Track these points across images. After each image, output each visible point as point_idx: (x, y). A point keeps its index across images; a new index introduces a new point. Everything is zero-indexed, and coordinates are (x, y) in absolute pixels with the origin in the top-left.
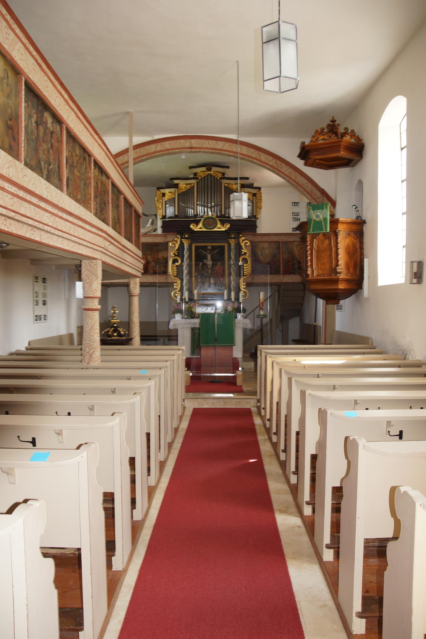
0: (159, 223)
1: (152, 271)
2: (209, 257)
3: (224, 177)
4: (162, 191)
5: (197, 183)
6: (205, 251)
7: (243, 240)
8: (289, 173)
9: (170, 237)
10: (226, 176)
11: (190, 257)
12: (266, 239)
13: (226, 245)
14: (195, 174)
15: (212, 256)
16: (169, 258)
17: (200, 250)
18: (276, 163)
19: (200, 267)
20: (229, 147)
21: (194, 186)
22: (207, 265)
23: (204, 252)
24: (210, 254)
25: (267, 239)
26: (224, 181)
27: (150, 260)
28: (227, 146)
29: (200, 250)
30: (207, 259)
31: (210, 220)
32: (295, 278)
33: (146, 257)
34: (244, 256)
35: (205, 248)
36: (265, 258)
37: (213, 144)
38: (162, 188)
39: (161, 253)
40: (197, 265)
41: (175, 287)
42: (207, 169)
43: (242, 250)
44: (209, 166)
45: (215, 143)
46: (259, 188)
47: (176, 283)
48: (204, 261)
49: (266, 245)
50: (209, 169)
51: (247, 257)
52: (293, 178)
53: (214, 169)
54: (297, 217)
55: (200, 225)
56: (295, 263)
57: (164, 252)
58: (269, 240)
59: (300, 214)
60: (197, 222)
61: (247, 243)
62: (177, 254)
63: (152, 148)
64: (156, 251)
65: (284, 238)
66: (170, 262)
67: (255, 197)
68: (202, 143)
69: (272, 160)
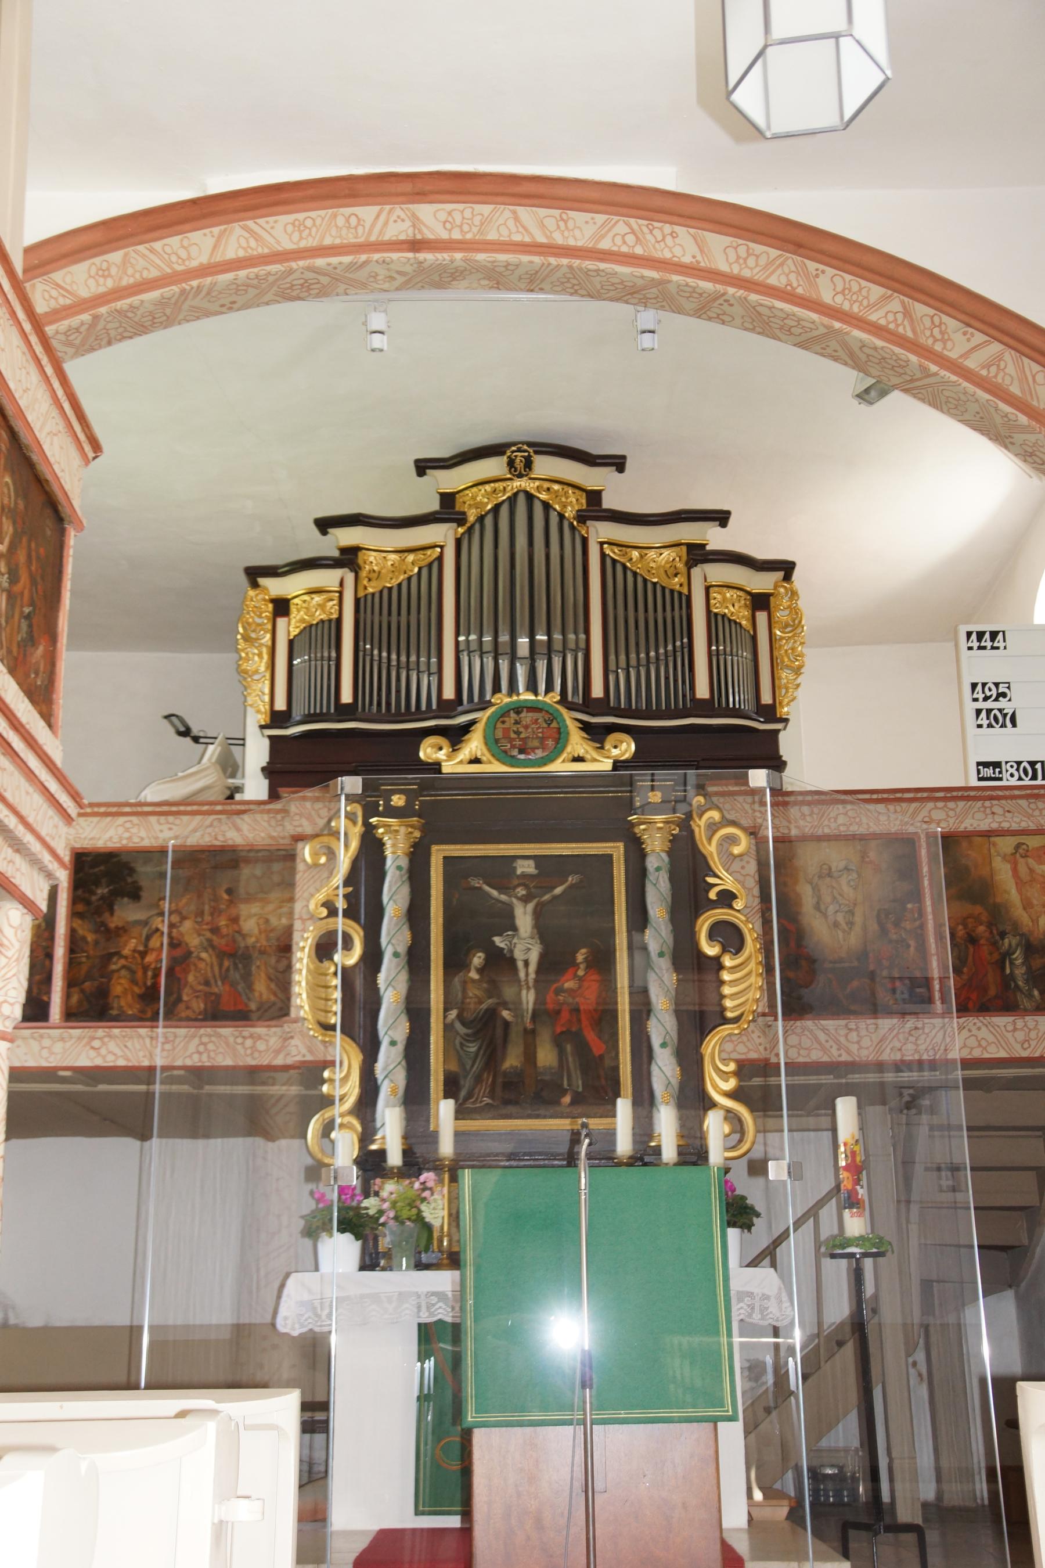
1: (199, 1005)
2: (524, 918)
3: (594, 506)
4: (276, 587)
5: (458, 542)
6: (501, 889)
7: (713, 828)
8: (988, 367)
9: (304, 809)
11: (416, 914)
12: (840, 819)
13: (617, 850)
14: (448, 499)
15: (537, 914)
16: (298, 925)
17: (476, 883)
18: (907, 313)
19: (474, 975)
20: (630, 239)
21: (440, 559)
22: (512, 961)
23: (495, 893)
24: (530, 906)
25: (841, 820)
26: (601, 531)
27: (194, 941)
28: (618, 233)
29: (476, 883)
30: (515, 929)
31: (527, 717)
32: (1020, 1035)
34: (720, 914)
35: (500, 872)
37: (542, 226)
38: (272, 572)
39: (255, 908)
42: (511, 463)
44: (519, 453)
45: (550, 223)
46: (787, 568)
48: (497, 940)
49: (836, 856)
50: (519, 464)
51: (738, 919)
52: (1015, 389)
53: (546, 466)
54: (1003, 703)
55: (474, 744)
56: (1009, 953)
58: (854, 829)
59: (1012, 694)
60: (456, 736)
61: (732, 840)
63: (199, 246)
64: (229, 891)
65: (938, 815)
66: (303, 958)
67: (762, 617)
68: (477, 220)
69: (885, 299)
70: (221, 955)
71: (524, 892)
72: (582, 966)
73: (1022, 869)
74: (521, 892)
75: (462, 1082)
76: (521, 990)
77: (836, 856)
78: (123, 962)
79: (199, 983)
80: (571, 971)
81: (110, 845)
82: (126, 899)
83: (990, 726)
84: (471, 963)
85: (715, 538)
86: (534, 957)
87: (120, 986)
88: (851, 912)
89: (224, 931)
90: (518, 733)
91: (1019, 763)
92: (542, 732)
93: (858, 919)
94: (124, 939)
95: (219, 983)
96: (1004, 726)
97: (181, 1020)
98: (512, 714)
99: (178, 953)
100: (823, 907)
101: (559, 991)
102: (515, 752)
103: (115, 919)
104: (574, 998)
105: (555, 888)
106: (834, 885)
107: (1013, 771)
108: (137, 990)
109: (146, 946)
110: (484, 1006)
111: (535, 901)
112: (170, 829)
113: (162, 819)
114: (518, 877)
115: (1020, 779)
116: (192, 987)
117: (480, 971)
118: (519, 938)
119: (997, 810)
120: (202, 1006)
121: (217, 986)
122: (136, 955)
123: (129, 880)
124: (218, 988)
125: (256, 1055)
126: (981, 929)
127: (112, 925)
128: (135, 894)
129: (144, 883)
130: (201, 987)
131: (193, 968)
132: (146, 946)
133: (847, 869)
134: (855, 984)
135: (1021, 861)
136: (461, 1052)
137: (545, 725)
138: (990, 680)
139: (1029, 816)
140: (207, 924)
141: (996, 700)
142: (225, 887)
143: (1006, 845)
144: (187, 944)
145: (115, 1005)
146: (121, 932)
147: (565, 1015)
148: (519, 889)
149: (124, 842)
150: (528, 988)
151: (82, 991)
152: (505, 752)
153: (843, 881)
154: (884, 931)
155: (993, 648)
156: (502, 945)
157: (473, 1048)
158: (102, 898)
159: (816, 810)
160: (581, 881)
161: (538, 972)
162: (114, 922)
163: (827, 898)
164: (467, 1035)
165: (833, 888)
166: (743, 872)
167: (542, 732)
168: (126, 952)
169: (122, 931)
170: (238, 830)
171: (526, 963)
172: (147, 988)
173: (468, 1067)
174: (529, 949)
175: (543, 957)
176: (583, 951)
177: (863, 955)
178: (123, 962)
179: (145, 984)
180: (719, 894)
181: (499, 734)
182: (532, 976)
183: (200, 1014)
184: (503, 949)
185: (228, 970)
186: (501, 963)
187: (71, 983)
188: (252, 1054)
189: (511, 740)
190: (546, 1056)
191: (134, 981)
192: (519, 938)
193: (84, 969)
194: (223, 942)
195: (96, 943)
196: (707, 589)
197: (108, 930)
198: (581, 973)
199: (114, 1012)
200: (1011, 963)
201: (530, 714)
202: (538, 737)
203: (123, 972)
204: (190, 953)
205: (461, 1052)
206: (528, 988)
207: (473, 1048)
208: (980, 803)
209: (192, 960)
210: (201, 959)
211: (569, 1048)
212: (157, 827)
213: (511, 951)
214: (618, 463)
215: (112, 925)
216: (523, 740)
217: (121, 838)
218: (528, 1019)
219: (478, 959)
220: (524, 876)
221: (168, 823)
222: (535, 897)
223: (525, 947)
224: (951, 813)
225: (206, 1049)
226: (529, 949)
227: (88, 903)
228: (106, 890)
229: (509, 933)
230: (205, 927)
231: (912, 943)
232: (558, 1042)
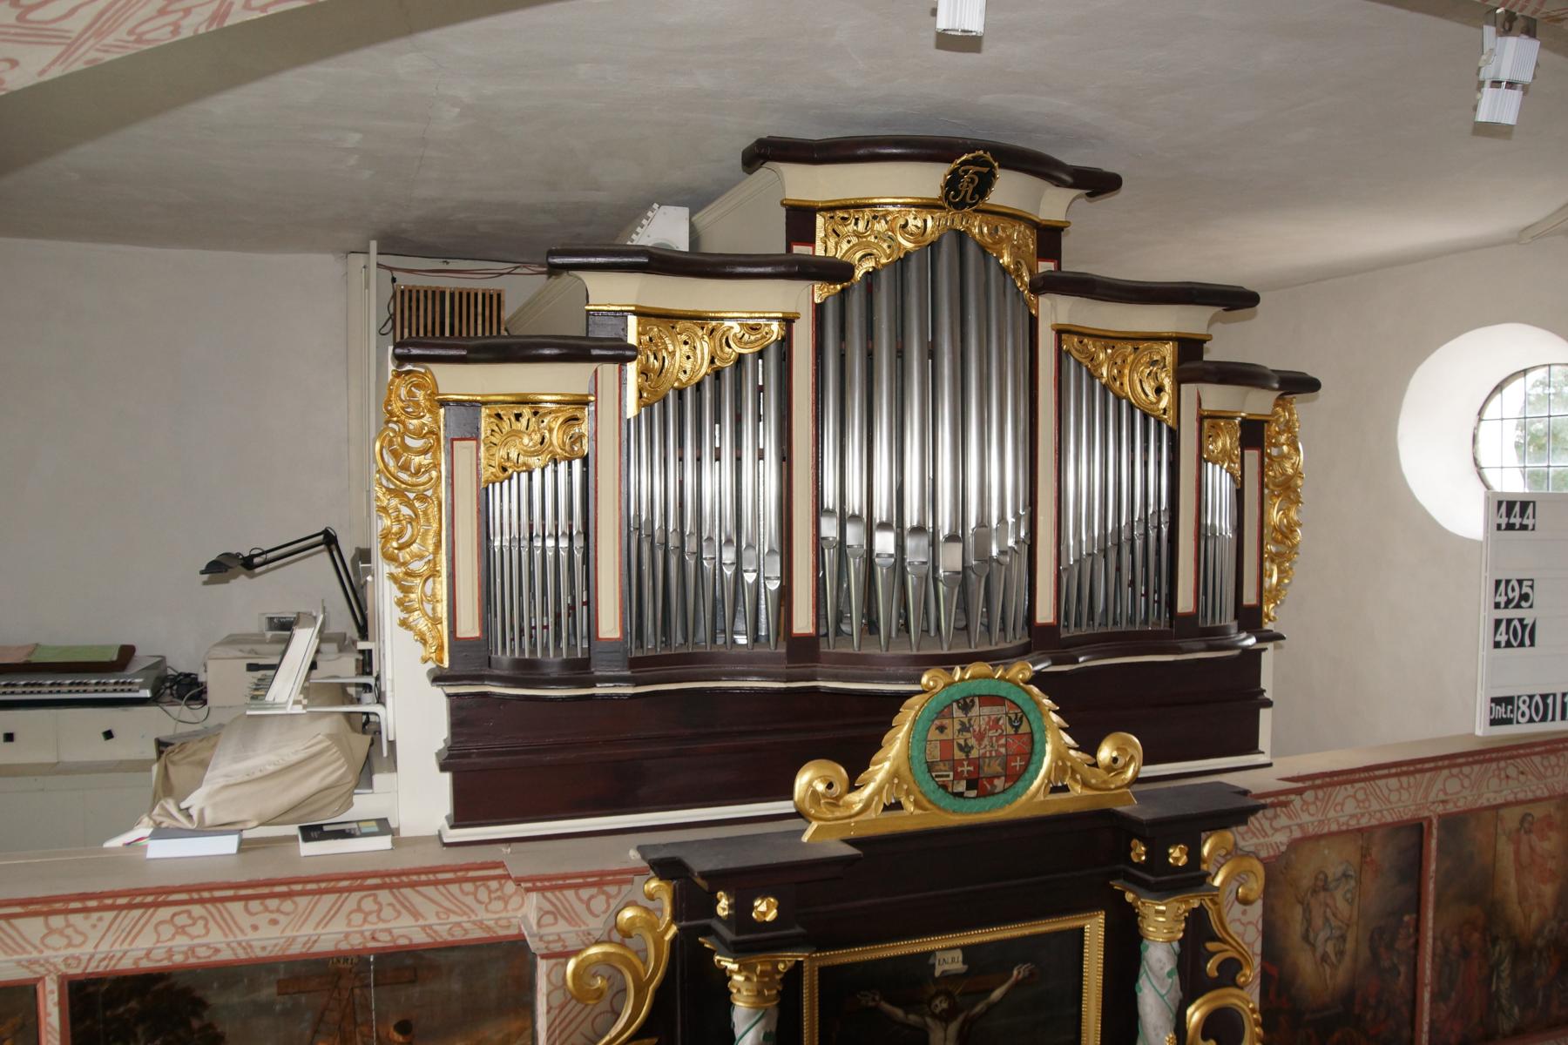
0: (417, 716)
5: (819, 310)
6: (908, 1004)
10: (1075, 260)
13: (1094, 927)
14: (800, 220)
23: (899, 1013)
25: (1350, 807)
31: (981, 715)
36: (1324, 958)
43: (1211, 946)
50: (966, 185)
53: (1008, 189)
59: (1536, 597)
65: (1453, 786)
67: (1252, 456)
71: (945, 1005)
73: (1525, 850)
77: (1334, 860)
81: (145, 964)
83: (1509, 644)
85: (1229, 341)
88: (1343, 938)
90: (966, 749)
91: (1531, 697)
92: (1005, 746)
93: (1350, 946)
96: (1522, 644)
98: (957, 713)
100: (1312, 935)
102: (961, 787)
105: (993, 990)
106: (1329, 901)
107: (1524, 708)
111: (961, 1018)
112: (274, 922)
113: (255, 905)
114: (936, 981)
115: (1531, 720)
119: (1512, 772)
123: (196, 1024)
126: (1476, 936)
133: (1345, 876)
135: (1525, 838)
137: (1011, 731)
138: (1514, 576)
139: (1541, 777)
141: (1518, 606)
142: (394, 1022)
143: (1511, 817)
149: (178, 959)
152: (944, 787)
153: (1339, 895)
154: (1375, 956)
155: (1524, 527)
159: (1320, 793)
160: (1032, 974)
163: (1318, 921)
165: (1327, 905)
166: (1245, 919)
167: (1005, 746)
170: (416, 915)
177: (1348, 997)
180: (1220, 967)
181: (936, 754)
189: (955, 765)
196: (1201, 419)
200: (1499, 977)
201: (986, 710)
202: (999, 755)
208: (1494, 765)
212: (245, 921)
214: (1098, 184)
216: (977, 764)
217: (170, 952)
220: (948, 977)
221: (267, 909)
224: (1466, 783)
231: (1402, 969)
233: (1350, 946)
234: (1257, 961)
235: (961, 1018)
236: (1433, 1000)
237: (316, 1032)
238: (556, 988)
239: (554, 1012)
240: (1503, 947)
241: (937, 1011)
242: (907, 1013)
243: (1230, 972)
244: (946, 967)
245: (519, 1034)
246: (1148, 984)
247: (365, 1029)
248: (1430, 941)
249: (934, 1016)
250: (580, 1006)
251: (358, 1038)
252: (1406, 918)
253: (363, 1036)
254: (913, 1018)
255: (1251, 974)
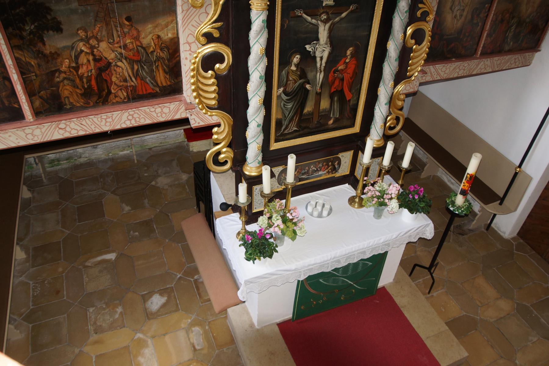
1: (123, 94)
2: (323, 33)
15: (331, 30)
17: (299, 13)
19: (293, 68)
22: (315, 57)
23: (309, 19)
24: (328, 25)
27: (111, 56)
29: (299, 13)
30: (318, 39)
33: (92, 48)
40: (285, 62)
41: (215, 137)
43: (420, 6)
47: (219, 125)
48: (308, 47)
57: (162, 21)
62: (216, 34)
64: (128, 19)
70: (131, 62)
71: (325, 17)
72: (349, 57)
74: (324, 17)
75: (283, 123)
76: (317, 73)
78: (63, 75)
79: (121, 81)
80: (343, 60)
82: (51, 32)
84: (292, 61)
86: (326, 55)
87: (66, 91)
88: (463, 10)
89: (131, 46)
93: (465, 14)
94: (59, 60)
95: (134, 79)
97: (113, 104)
99: (102, 64)
100: (453, 7)
101: (336, 71)
103: (47, 47)
104: (342, 74)
108: (79, 91)
109: (77, 63)
110: (297, 84)
111: (331, 22)
114: (323, 7)
116: (115, 84)
117: (297, 66)
118: (320, 45)
120: (125, 94)
121: (132, 81)
122: (72, 70)
123: (49, 17)
124: (134, 82)
125: (164, 115)
126: (508, 15)
127: (48, 52)
128: (58, 28)
129: (61, 19)
130: (121, 84)
131: (114, 72)
132: (77, 63)
134: (453, 45)
136: (284, 108)
140: (117, 43)
142: (124, 17)
144: (106, 58)
145: (67, 102)
146: (55, 56)
147: (337, 83)
148: (323, 16)
150: (321, 72)
151: (41, 97)
156: (310, 50)
157: (290, 106)
158: (31, 32)
160: (357, 8)
161: (326, 63)
162: (48, 50)
164: (287, 100)
168: (63, 68)
169: (55, 55)
171: (321, 58)
172: (85, 89)
173: (287, 115)
174: (324, 50)
175: (330, 54)
176: (351, 48)
178: (63, 75)
179: (83, 87)
182: (324, 65)
183: (125, 98)
184: (310, 52)
185: (138, 70)
186: (309, 59)
187: (30, 94)
188: (161, 115)
190: (325, 104)
191: (75, 86)
192: (320, 45)
193: (37, 84)
194: (131, 54)
195: (39, 65)
197: (45, 56)
198: (347, 61)
199: (68, 107)
203: (66, 82)
204: (109, 64)
205: (284, 108)
206: (321, 72)
207: (290, 106)
209: (112, 68)
210: (118, 66)
211: (336, 98)
213: (315, 53)
215: (48, 52)
218: (318, 88)
219: (296, 59)
220: (328, 7)
222: (331, 20)
223: (322, 51)
225: (133, 117)
226: (324, 50)
227: (22, 38)
228: (33, 27)
229: (315, 42)
230: (116, 45)
231: (480, 24)
232: (331, 97)
233: (465, 14)
234: (434, 13)
235: (331, 22)
236: (487, 37)
237: (96, 20)
238: (185, 3)
239: (185, 12)
240: (515, 20)
241: (322, 19)
242: (312, 19)
243: (425, 14)
244: (327, 3)
245: (172, 21)
246: (397, 15)
247: (114, 19)
248: (492, 15)
249: (322, 21)
250: (194, 9)
251: (112, 23)
252: (486, 6)
253: (114, 22)
254: (314, 21)
255: (431, 17)
